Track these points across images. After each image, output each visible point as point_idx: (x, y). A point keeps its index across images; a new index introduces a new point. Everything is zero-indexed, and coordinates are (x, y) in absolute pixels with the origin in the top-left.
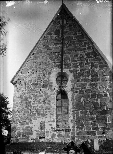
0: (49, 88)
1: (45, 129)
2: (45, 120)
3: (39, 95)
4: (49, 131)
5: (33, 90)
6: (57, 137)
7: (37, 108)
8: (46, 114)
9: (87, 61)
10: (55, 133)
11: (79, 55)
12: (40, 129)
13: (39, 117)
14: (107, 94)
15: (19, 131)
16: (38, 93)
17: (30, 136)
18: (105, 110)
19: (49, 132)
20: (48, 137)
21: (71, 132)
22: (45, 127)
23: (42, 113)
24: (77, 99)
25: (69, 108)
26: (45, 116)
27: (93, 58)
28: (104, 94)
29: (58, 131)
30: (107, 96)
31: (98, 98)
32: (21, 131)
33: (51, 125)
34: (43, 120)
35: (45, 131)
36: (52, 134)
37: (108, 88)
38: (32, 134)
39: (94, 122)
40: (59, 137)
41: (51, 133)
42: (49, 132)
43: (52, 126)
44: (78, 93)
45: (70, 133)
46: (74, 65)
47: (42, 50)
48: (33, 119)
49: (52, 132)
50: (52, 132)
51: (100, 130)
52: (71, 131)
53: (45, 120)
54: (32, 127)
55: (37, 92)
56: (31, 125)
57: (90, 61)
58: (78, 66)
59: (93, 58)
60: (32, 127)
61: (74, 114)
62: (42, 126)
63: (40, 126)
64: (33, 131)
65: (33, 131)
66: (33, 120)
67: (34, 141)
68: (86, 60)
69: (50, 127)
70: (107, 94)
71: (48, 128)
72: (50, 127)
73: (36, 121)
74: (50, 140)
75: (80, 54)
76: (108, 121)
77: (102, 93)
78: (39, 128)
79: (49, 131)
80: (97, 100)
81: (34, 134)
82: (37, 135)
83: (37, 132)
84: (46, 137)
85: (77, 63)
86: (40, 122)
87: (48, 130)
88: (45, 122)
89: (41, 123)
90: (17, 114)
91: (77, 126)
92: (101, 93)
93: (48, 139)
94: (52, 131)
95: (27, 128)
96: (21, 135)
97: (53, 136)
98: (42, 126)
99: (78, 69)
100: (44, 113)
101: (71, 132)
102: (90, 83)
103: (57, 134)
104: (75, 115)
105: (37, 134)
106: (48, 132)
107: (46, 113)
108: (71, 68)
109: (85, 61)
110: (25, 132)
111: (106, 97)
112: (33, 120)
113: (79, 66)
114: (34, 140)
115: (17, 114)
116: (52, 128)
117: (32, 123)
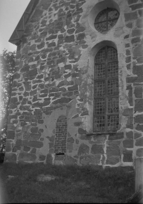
0: (78, 41)
1: (66, 134)
2: (67, 113)
3: (58, 58)
4: (75, 140)
6: (90, 153)
7: (53, 87)
8: (70, 100)
10: (86, 142)
12: (56, 135)
13: (55, 108)
15: (19, 138)
16: (57, 56)
17: (37, 149)
19: (75, 142)
21: (124, 139)
22: (66, 130)
25: (119, 79)
26: (67, 104)
32: (23, 139)
34: (64, 113)
35: (65, 138)
36: (79, 145)
38: (41, 145)
40: (95, 153)
41: (77, 142)
42: (75, 142)
45: (122, 144)
48: (44, 112)
49: (80, 140)
50: (81, 142)
52: (122, 137)
53: (67, 113)
54: (42, 130)
55: (54, 54)
56: (40, 126)
60: (42, 130)
61: (130, 94)
63: (57, 127)
64: (42, 139)
65: (42, 139)
66: (44, 115)
67: (45, 161)
69: (77, 128)
71: (72, 131)
72: (77, 128)
74: (75, 158)
78: (54, 132)
79: (75, 138)
81: (44, 145)
82: (50, 147)
83: (50, 142)
84: (68, 153)
86: (57, 119)
87: (73, 136)
88: (66, 118)
89: (58, 121)
91: (136, 124)
93: (71, 157)
94: (82, 138)
95: (34, 130)
96: (22, 148)
97: (83, 149)
100: (66, 97)
101: (124, 139)
103: (90, 146)
104: (134, 95)
105: (51, 145)
106: (71, 140)
107: (71, 97)
110: (29, 141)
112: (44, 115)
114: (44, 159)
116: (81, 131)
117: (42, 122)
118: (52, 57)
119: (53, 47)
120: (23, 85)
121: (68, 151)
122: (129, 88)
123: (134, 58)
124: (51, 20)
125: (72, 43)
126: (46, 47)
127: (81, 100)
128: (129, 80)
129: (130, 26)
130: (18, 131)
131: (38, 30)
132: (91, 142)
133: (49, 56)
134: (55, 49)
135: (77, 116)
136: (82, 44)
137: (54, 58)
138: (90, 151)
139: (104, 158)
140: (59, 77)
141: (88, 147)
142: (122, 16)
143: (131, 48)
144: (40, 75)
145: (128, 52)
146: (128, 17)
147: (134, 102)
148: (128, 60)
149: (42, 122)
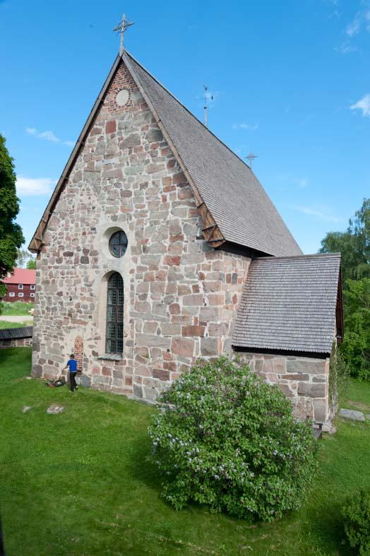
5: (65, 268)
6: (101, 374)
9: (164, 199)
11: (149, 185)
14: (198, 285)
18: (193, 325)
20: (86, 370)
21: (126, 366)
23: (78, 318)
24: (140, 294)
27: (177, 192)
28: (193, 286)
29: (103, 362)
30: (198, 291)
31: (180, 294)
33: (91, 347)
37: (203, 272)
39: (168, 350)
40: (104, 374)
43: (94, 349)
44: (142, 280)
46: (139, 210)
47: (83, 172)
51: (177, 370)
52: (125, 364)
57: (170, 199)
58: (147, 212)
59: (177, 192)
60: (63, 347)
62: (79, 345)
65: (63, 355)
68: (163, 196)
69: (91, 350)
70: (198, 285)
71: (87, 351)
73: (70, 335)
75: (152, 180)
76: (194, 352)
77: (188, 282)
78: (72, 349)
80: (177, 299)
84: (84, 372)
85: (144, 206)
87: (88, 357)
90: (41, 317)
92: (186, 282)
97: (96, 370)
98: (79, 345)
99: (145, 219)
100: (82, 319)
101: (126, 366)
102: (168, 256)
103: (101, 368)
104: (135, 329)
106: (86, 360)
108: (133, 218)
109: (161, 200)
111: (196, 294)
113: (148, 214)
115: (41, 317)
116: (95, 354)
117: (62, 339)
118: (69, 276)
119: (71, 265)
120: (45, 299)
121: (84, 369)
122: (131, 321)
123: (137, 294)
124: (68, 233)
125: (87, 265)
126: (64, 263)
127: (95, 325)
128: (132, 314)
129: (135, 260)
130: (42, 345)
131: (56, 241)
132: (102, 365)
133: (67, 273)
134: (73, 268)
135: (90, 339)
136: (95, 269)
137: (71, 277)
138: (101, 372)
139: (111, 379)
140: (76, 298)
141: (99, 368)
142: (129, 246)
143: (136, 283)
144: (59, 291)
145: (132, 287)
146: (133, 249)
147: (135, 336)
148: (132, 295)
149: (62, 339)
